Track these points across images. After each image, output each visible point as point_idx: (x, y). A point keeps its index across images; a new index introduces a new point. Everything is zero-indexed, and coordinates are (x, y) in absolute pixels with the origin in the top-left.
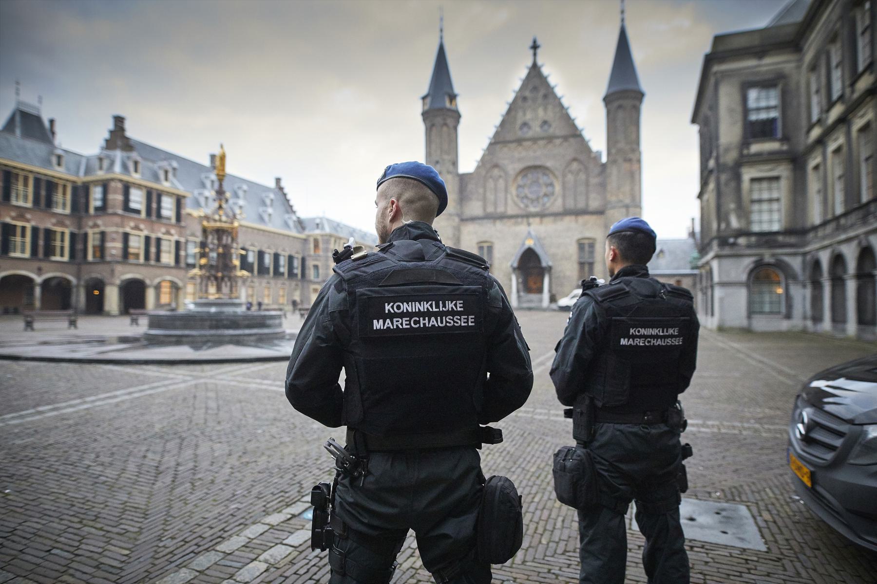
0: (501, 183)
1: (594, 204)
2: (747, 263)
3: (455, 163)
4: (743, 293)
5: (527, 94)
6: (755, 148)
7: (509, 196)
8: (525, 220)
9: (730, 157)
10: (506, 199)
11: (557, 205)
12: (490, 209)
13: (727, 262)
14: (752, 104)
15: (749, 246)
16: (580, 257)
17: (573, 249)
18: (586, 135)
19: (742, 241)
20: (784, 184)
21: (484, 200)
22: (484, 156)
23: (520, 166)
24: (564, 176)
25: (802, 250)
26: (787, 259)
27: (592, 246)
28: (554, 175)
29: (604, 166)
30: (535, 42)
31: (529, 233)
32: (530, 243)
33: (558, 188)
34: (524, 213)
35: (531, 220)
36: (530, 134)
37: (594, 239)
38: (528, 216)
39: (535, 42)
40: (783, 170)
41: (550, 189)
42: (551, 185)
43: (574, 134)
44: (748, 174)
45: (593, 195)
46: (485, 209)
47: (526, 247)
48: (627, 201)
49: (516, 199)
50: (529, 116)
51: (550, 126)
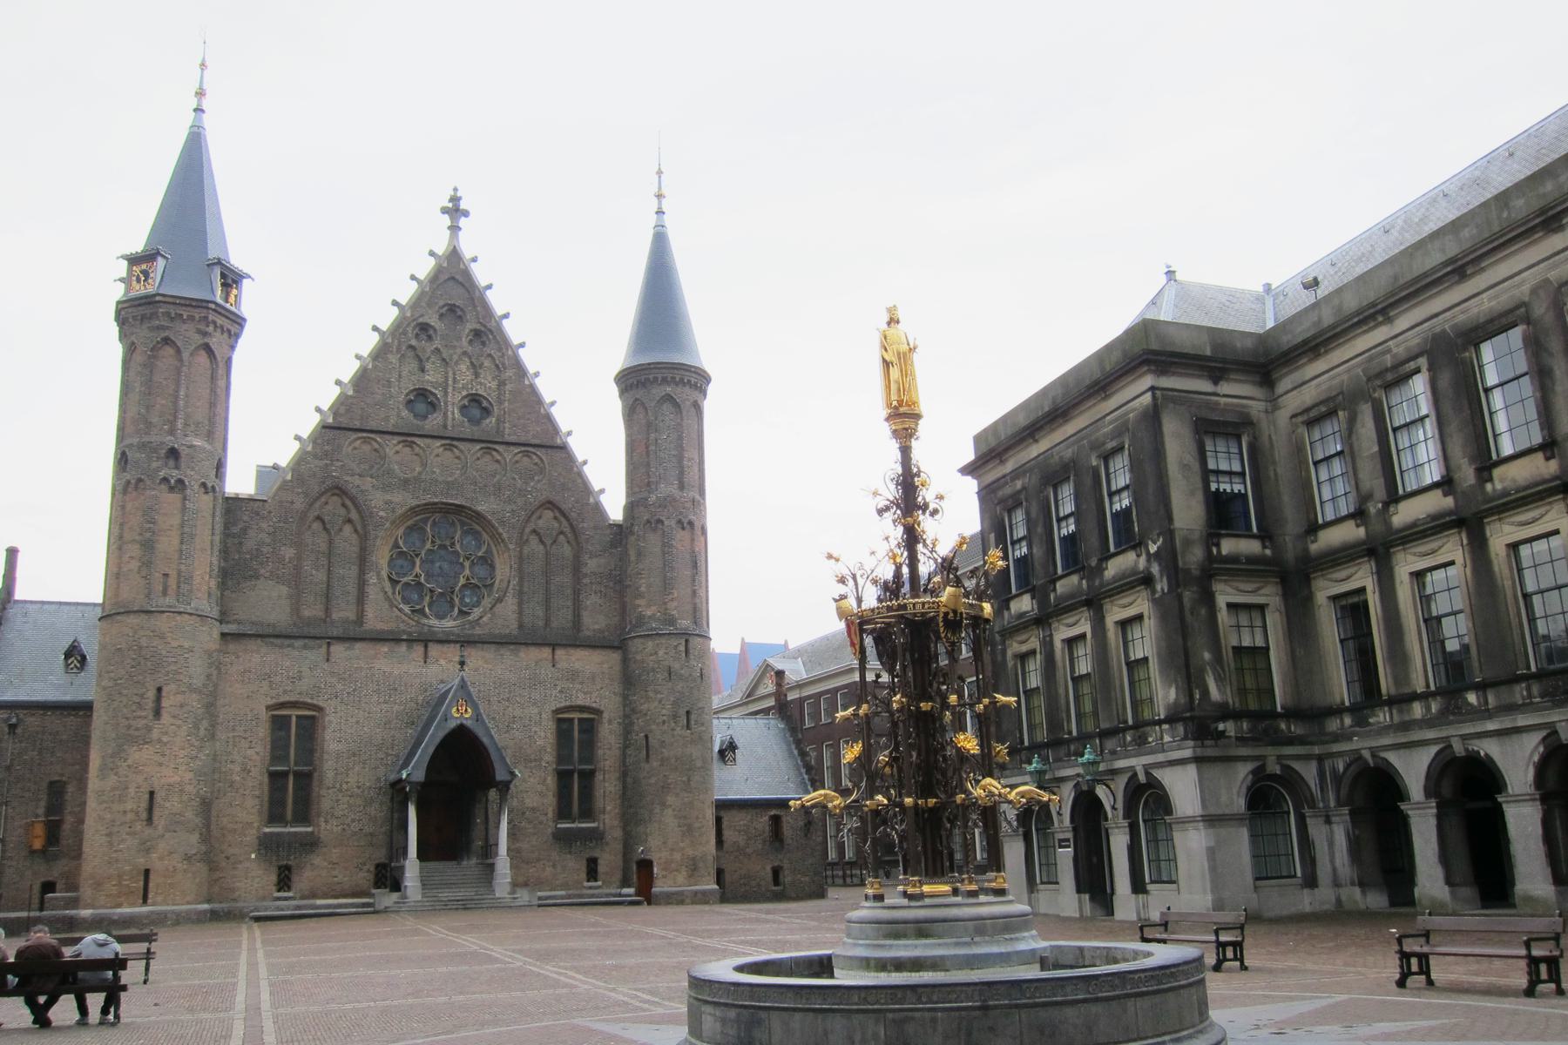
0: (347, 540)
1: (596, 620)
2: (1243, 771)
3: (220, 467)
4: (1244, 833)
5: (433, 320)
6: (1228, 546)
7: (372, 579)
8: (419, 649)
9: (1194, 557)
10: (362, 584)
11: (506, 616)
12: (312, 610)
13: (1214, 771)
14: (1212, 465)
15: (1241, 740)
16: (560, 759)
17: (544, 736)
18: (579, 447)
19: (1228, 727)
20: (1274, 620)
21: (296, 581)
22: (300, 460)
23: (403, 500)
24: (522, 542)
25: (1316, 750)
26: (1296, 765)
27: (589, 727)
28: (497, 538)
29: (620, 533)
30: (455, 199)
31: (463, 685)
32: (460, 714)
33: (504, 570)
34: (409, 625)
35: (434, 650)
36: (433, 422)
37: (598, 712)
38: (426, 640)
39: (455, 199)
40: (1269, 595)
41: (481, 571)
42: (487, 561)
43: (548, 447)
44: (1225, 594)
45: (591, 600)
46: (296, 610)
47: (452, 724)
48: (685, 623)
49: (387, 584)
50: (432, 377)
51: (487, 412)
